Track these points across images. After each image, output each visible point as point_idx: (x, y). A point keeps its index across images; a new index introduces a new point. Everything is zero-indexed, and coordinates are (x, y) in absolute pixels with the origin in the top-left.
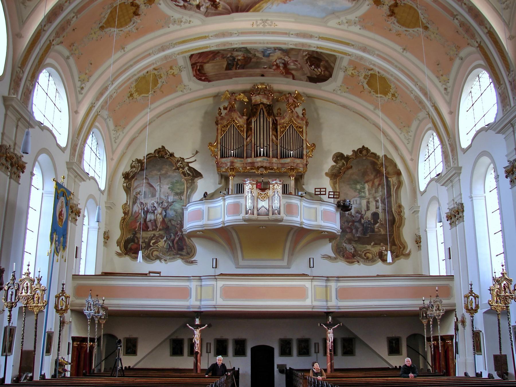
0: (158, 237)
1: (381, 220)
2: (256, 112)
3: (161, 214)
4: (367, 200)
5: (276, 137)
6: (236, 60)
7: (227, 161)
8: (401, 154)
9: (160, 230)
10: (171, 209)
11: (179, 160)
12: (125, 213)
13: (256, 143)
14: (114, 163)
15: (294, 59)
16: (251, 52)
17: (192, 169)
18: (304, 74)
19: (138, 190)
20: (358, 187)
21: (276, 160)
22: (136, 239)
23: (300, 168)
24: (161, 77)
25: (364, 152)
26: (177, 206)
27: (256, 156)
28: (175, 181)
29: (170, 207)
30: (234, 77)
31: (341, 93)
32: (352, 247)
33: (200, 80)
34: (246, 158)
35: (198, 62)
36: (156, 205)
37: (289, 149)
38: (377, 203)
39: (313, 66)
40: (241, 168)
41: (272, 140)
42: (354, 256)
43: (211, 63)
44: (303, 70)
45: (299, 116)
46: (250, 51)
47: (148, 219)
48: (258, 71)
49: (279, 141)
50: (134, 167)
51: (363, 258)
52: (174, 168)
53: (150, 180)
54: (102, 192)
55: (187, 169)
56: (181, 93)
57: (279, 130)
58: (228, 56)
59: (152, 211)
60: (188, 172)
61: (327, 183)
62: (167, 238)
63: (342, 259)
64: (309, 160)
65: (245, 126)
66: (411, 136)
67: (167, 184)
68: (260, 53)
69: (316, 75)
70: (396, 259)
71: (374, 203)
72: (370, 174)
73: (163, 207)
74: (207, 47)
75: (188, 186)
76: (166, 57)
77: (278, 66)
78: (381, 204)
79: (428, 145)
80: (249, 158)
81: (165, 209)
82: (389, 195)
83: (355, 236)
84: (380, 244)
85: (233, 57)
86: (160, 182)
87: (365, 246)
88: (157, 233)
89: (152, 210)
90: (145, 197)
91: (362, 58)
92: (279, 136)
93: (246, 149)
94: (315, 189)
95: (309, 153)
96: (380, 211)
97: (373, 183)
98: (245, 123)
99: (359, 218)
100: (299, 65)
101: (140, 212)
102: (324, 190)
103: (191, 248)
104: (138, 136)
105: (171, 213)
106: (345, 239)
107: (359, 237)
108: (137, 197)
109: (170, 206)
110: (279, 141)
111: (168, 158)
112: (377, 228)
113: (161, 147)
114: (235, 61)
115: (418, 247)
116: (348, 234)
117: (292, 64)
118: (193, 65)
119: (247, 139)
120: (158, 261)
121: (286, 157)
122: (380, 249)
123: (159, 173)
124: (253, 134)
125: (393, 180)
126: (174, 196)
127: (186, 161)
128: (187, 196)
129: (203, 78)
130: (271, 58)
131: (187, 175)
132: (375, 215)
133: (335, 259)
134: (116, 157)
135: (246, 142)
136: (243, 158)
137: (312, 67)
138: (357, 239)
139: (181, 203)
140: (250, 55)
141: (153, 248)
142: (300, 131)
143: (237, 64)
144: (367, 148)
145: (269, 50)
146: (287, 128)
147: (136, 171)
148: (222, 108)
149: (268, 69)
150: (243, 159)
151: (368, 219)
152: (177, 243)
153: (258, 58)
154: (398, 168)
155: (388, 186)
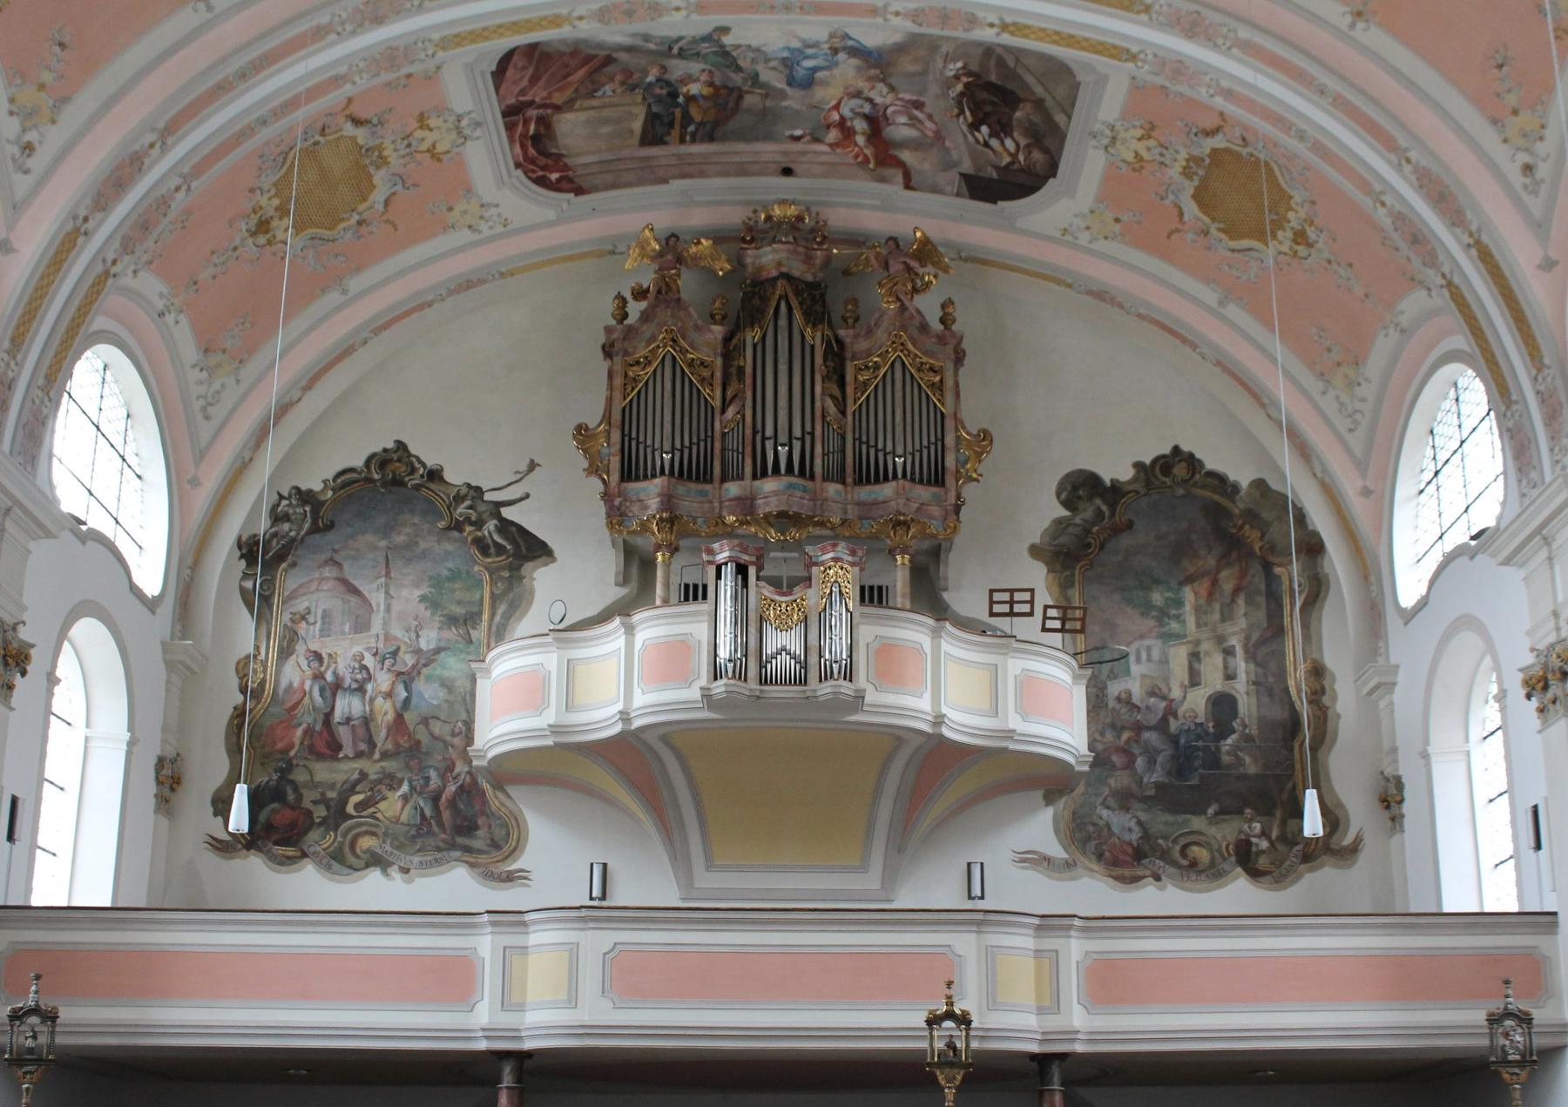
0: (379, 781)
1: (1243, 721)
2: (761, 311)
3: (389, 695)
4: (1190, 646)
6: (681, 100)
7: (650, 493)
9: (385, 755)
10: (429, 679)
13: (759, 427)
14: (202, 499)
15: (907, 97)
16: (741, 63)
17: (514, 529)
19: (301, 605)
20: (1157, 598)
21: (838, 492)
22: (289, 790)
23: (933, 522)
24: (383, 161)
26: (452, 666)
27: (760, 473)
28: (445, 573)
29: (425, 671)
30: (674, 177)
32: (1133, 824)
33: (542, 182)
34: (724, 479)
35: (531, 103)
36: (369, 661)
37: (889, 448)
38: (1230, 659)
39: (985, 129)
40: (699, 521)
41: (824, 417)
42: (1139, 855)
43: (581, 109)
44: (947, 143)
46: (735, 60)
47: (338, 715)
48: (769, 151)
49: (850, 418)
50: (286, 517)
51: (1174, 864)
52: (442, 524)
53: (346, 566)
55: (492, 528)
56: (465, 236)
57: (849, 378)
58: (650, 78)
59: (354, 686)
60: (497, 538)
61: (1036, 576)
62: (412, 788)
63: (1095, 866)
64: (969, 491)
65: (719, 362)
66: (1363, 400)
67: (417, 585)
68: (773, 68)
73: (399, 668)
75: (496, 592)
77: (847, 132)
79: (1432, 432)
80: (733, 479)
81: (407, 678)
83: (1145, 780)
85: (668, 84)
86: (387, 575)
87: (1180, 818)
88: (373, 769)
89: (356, 681)
90: (325, 632)
92: (850, 401)
93: (723, 449)
95: (968, 466)
96: (1240, 688)
98: (719, 351)
99: (1160, 715)
100: (929, 125)
101: (307, 688)
104: (299, 400)
105: (429, 693)
106: (1107, 792)
108: (296, 633)
109: (425, 665)
110: (850, 418)
111: (417, 487)
112: (1228, 753)
113: (390, 445)
114: (678, 105)
116: (1119, 773)
117: (903, 119)
119: (723, 411)
121: (877, 481)
123: (383, 543)
124: (749, 394)
126: (439, 628)
127: (488, 497)
128: (494, 629)
129: (554, 176)
130: (819, 93)
131: (492, 550)
132: (1223, 705)
133: (1069, 865)
134: (213, 476)
135: (721, 421)
136: (711, 481)
137: (979, 131)
139: (468, 653)
140: (737, 79)
142: (933, 384)
143: (687, 119)
145: (810, 51)
146: (883, 371)
147: (293, 534)
148: (628, 295)
149: (809, 142)
150: (708, 487)
151: (1196, 717)
153: (768, 91)
154: (1311, 528)
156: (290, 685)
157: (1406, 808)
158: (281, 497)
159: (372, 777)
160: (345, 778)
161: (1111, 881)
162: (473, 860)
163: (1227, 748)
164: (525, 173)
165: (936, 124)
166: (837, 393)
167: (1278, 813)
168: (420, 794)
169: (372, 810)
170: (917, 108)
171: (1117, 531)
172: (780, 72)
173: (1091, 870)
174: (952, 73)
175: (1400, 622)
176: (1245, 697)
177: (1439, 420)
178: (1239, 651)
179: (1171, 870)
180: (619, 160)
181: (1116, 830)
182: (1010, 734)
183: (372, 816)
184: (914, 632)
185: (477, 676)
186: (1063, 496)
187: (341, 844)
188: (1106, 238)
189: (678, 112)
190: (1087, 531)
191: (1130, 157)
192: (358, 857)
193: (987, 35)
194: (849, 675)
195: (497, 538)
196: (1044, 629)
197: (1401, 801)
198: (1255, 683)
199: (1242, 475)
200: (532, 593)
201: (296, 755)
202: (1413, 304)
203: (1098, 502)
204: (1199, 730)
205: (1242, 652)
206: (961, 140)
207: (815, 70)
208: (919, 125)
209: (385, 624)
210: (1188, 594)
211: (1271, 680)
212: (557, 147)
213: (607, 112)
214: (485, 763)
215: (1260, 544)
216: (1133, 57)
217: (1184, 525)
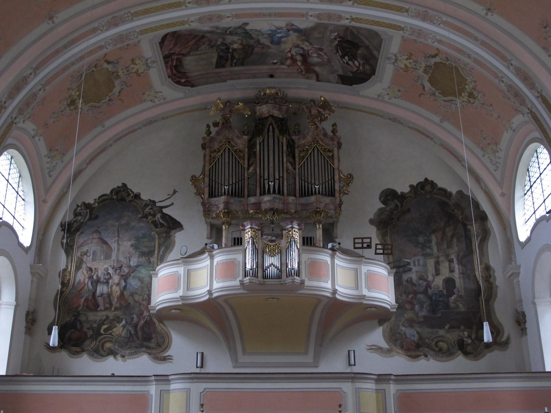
0: (114, 320)
1: (458, 289)
3: (118, 284)
5: (293, 165)
6: (231, 50)
7: (220, 202)
8: (486, 186)
9: (116, 309)
10: (134, 277)
11: (148, 203)
12: (63, 284)
13: (262, 174)
14: (47, 208)
15: (317, 46)
16: (253, 36)
17: (167, 217)
19: (85, 249)
20: (421, 239)
21: (293, 200)
22: (78, 324)
23: (331, 211)
24: (118, 77)
25: (428, 188)
26: (143, 272)
27: (263, 193)
28: (141, 235)
29: (132, 275)
30: (228, 80)
31: (389, 99)
32: (415, 333)
33: (178, 83)
34: (248, 196)
35: (174, 53)
36: (111, 271)
37: (313, 182)
38: (452, 264)
39: (346, 58)
40: (240, 213)
41: (287, 171)
42: (418, 346)
43: (193, 55)
44: (332, 64)
45: (327, 133)
46: (251, 35)
47: (98, 293)
49: (297, 171)
50: (80, 214)
51: (432, 349)
52: (140, 216)
53: (102, 234)
54: (26, 250)
55: (159, 217)
56: (150, 104)
58: (219, 43)
59: (105, 281)
60: (161, 220)
61: (372, 233)
62: (126, 322)
63: (400, 351)
64: (345, 198)
65: (246, 150)
66: (499, 158)
67: (130, 240)
68: (265, 38)
69: (352, 72)
70: (486, 350)
71: (447, 264)
73: (122, 273)
74: (183, 23)
75: (161, 242)
76: (121, 37)
78: (458, 264)
79: (528, 170)
80: (252, 196)
81: (125, 277)
83: (419, 315)
84: (459, 328)
85: (226, 45)
86: (118, 236)
87: (435, 330)
88: (111, 314)
89: (105, 279)
90: (94, 260)
91: (420, 32)
92: (297, 164)
93: (248, 184)
94: (354, 239)
95: (344, 188)
96: (456, 275)
97: (444, 233)
98: (246, 146)
99: (424, 288)
100: (325, 57)
101: (86, 282)
102: (368, 240)
103: (163, 337)
104: (86, 168)
105: (134, 283)
106: (404, 320)
107: (425, 317)
108: (82, 260)
109: (132, 272)
110: (297, 171)
111: (130, 201)
112: (453, 303)
113: (120, 185)
114: (230, 52)
115: (522, 330)
116: (408, 312)
117: (315, 55)
118: (167, 58)
119: (248, 169)
120: (111, 359)
121: (308, 195)
122: (459, 336)
123: (117, 224)
124: (258, 162)
125: (474, 228)
126: (138, 257)
127: (158, 204)
128: (159, 257)
129: (183, 80)
130: (283, 46)
131: (159, 226)
132: (449, 282)
133: (389, 351)
135: (247, 173)
136: (244, 197)
137: (344, 59)
138: (421, 320)
139: (149, 267)
140: (252, 42)
141: (105, 338)
142: (330, 156)
143: (233, 58)
144: (432, 182)
145: (279, 31)
146: (310, 152)
147: (82, 220)
150: (242, 199)
152: (142, 328)
153: (264, 46)
154: (481, 209)
156: (80, 280)
157: (528, 325)
158: (78, 206)
159: (111, 318)
160: (100, 318)
161: (407, 357)
162: (150, 352)
163: (452, 300)
164: (172, 80)
165: (328, 56)
166: (291, 160)
167: (475, 328)
168: (130, 324)
169: (110, 331)
170: (320, 51)
172: (268, 39)
173: (399, 353)
174: (333, 37)
175: (520, 248)
176: (458, 279)
177: (531, 165)
179: (431, 352)
180: (208, 74)
181: (408, 336)
182: (363, 297)
183: (111, 334)
184: (325, 257)
185: (153, 276)
186: (382, 199)
187: (98, 346)
188: (395, 98)
189: (229, 55)
191: (403, 66)
192: (104, 351)
193: (346, 22)
194: (298, 273)
195: (161, 220)
196: (376, 254)
197: (525, 322)
198: (462, 273)
199: (453, 189)
200: (174, 242)
201: (81, 309)
202: (518, 119)
203: (396, 201)
204: (440, 293)
205: (456, 261)
207: (281, 37)
209: (117, 256)
211: (469, 272)
214: (155, 312)
216: (402, 29)
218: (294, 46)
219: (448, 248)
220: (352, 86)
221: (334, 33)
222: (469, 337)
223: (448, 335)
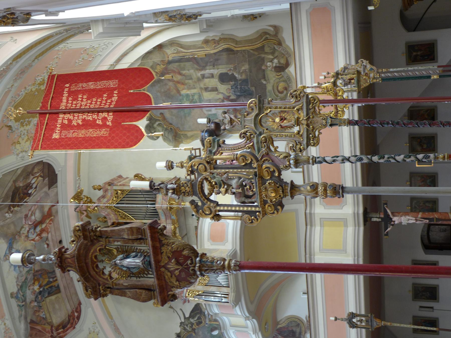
1: (229, 70)
4: (203, 91)
6: (41, 289)
8: (130, 49)
11: (183, 328)
15: (24, 221)
18: (47, 194)
33: (78, 318)
38: (206, 76)
45: (102, 196)
46: (23, 282)
52: (194, 334)
55: (193, 320)
57: (124, 221)
60: (196, 319)
70: (283, 45)
71: (206, 80)
72: (168, 87)
77: (42, 231)
78: (206, 70)
82: (194, 60)
84: (264, 70)
85: (37, 297)
96: (216, 72)
97: (178, 82)
100: (33, 209)
112: (241, 76)
114: (44, 289)
115: (260, 16)
122: (271, 70)
125: (170, 53)
127: (183, 320)
131: (200, 320)
132: (223, 78)
137: (31, 193)
149: (48, 241)
151: (229, 89)
155: (180, 60)
163: (239, 76)
164: (76, 324)
167: (263, 56)
170: (27, 216)
171: (164, 119)
174: (11, 214)
176: (219, 70)
178: (203, 72)
180: (67, 296)
189: (45, 288)
190: (166, 129)
195: (196, 319)
198: (214, 67)
204: (234, 87)
205: (202, 72)
206: (36, 196)
208: (34, 212)
210: (184, 92)
211: (212, 60)
212: (66, 319)
213: (51, 310)
215: (162, 66)
217: (159, 94)
218: (28, 239)
219: (191, 79)
220: (57, 174)
221: (5, 217)
222: (271, 61)
223: (272, 81)
